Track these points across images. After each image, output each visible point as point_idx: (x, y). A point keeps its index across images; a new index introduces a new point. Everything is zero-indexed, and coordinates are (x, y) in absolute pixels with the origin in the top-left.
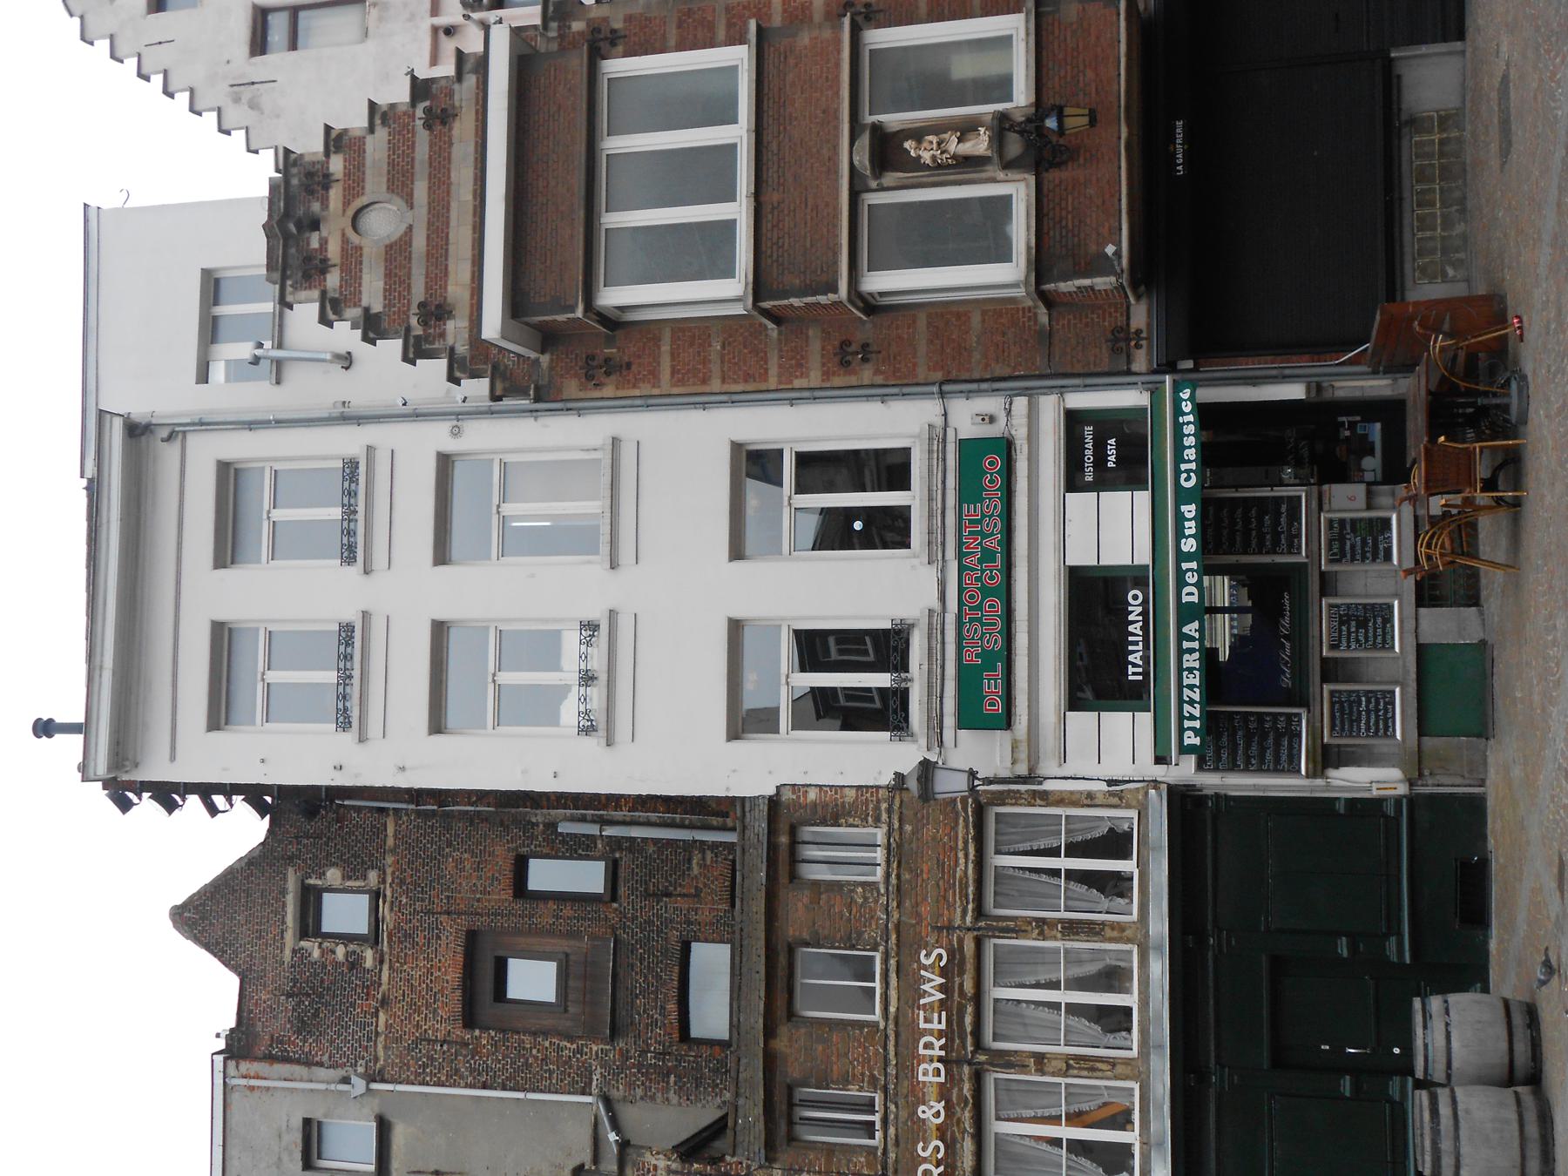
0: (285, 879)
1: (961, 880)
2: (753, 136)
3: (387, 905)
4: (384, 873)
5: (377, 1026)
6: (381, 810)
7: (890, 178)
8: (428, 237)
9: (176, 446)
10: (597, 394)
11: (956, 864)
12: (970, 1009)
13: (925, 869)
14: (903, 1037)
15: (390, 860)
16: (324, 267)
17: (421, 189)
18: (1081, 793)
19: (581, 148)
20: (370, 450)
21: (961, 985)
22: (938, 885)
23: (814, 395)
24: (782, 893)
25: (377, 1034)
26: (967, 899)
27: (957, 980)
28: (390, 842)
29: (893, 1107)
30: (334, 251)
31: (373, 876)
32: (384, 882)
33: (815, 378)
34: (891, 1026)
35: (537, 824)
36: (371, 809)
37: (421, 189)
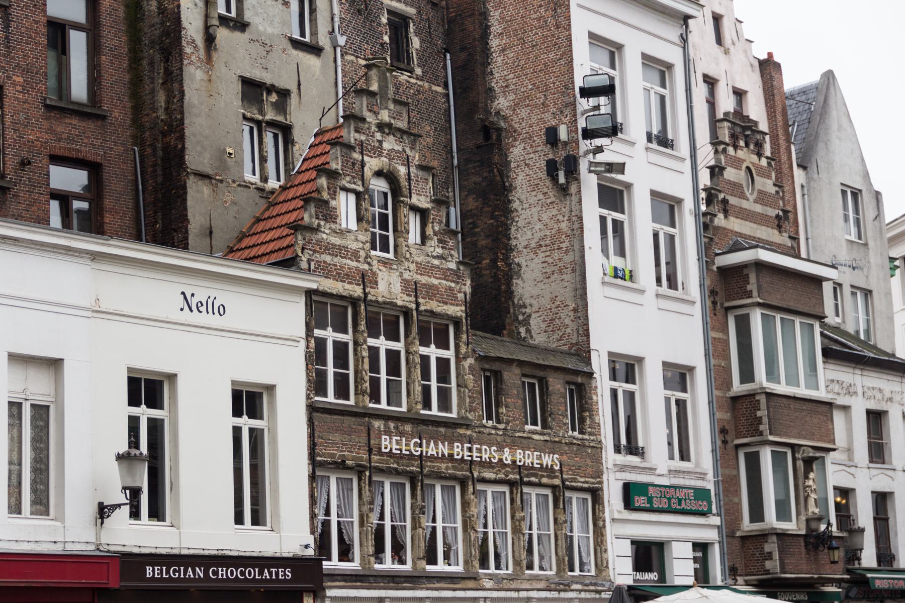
0: (412, 6)
1: (576, 479)
2: (809, 398)
3: (407, 78)
4: (421, 80)
5: (360, 58)
6: (446, 86)
7: (800, 464)
8: (746, 209)
9: (677, 40)
10: (707, 296)
11: (581, 477)
12: (537, 480)
13: (578, 459)
14: (523, 441)
15: (426, 85)
16: (736, 147)
17: (758, 208)
18: (606, 546)
19: (800, 308)
20: (683, 160)
21: (543, 476)
22: (573, 466)
23: (712, 415)
24: (561, 376)
25: (357, 57)
26: (571, 482)
27: (545, 474)
28: (434, 88)
29: (501, 433)
30: (741, 154)
31: (418, 71)
32: (417, 79)
33: (718, 415)
34: (525, 435)
35: (448, 192)
36: (446, 77)
37: (758, 208)
